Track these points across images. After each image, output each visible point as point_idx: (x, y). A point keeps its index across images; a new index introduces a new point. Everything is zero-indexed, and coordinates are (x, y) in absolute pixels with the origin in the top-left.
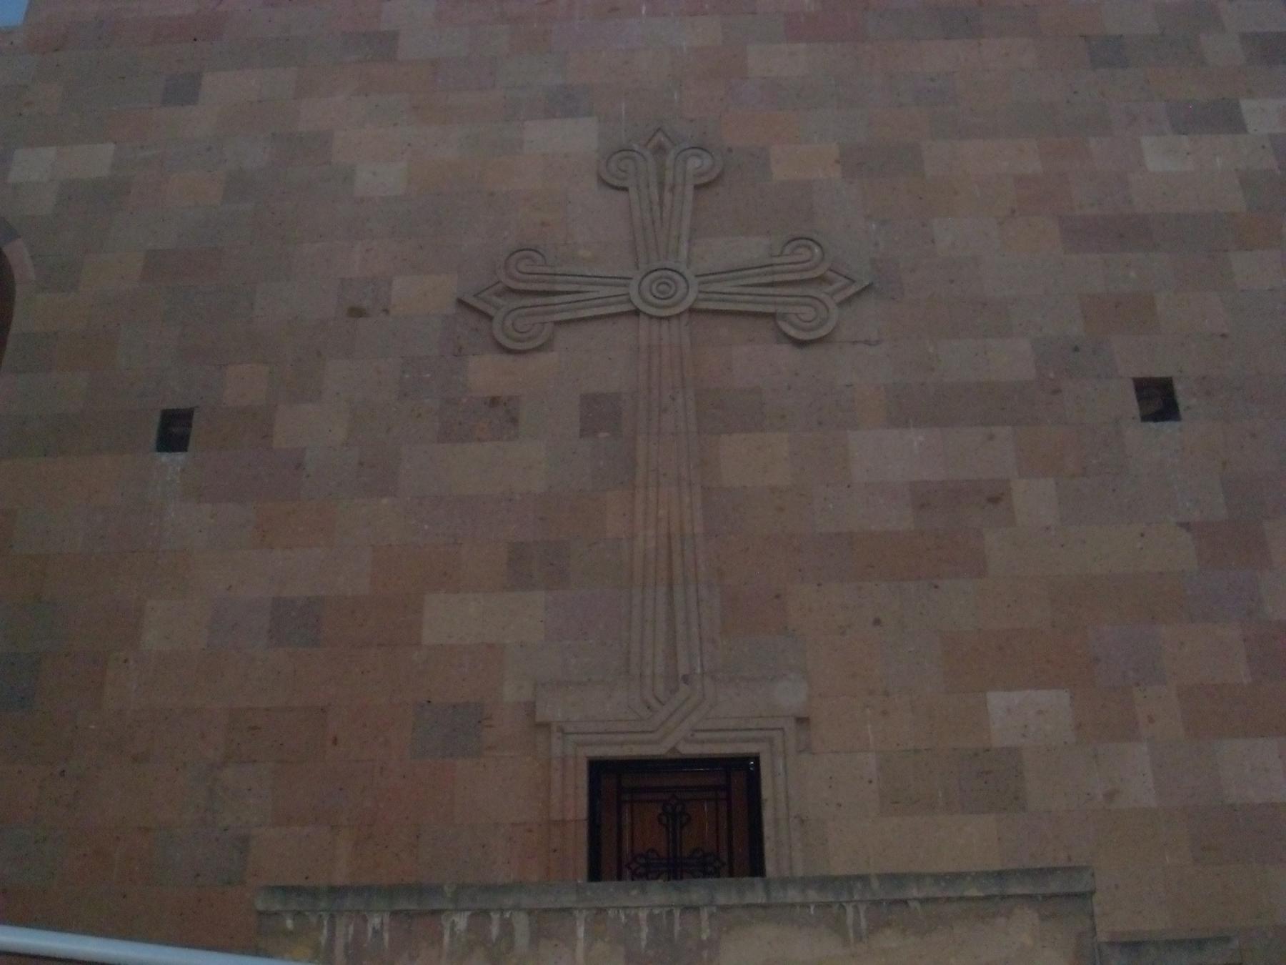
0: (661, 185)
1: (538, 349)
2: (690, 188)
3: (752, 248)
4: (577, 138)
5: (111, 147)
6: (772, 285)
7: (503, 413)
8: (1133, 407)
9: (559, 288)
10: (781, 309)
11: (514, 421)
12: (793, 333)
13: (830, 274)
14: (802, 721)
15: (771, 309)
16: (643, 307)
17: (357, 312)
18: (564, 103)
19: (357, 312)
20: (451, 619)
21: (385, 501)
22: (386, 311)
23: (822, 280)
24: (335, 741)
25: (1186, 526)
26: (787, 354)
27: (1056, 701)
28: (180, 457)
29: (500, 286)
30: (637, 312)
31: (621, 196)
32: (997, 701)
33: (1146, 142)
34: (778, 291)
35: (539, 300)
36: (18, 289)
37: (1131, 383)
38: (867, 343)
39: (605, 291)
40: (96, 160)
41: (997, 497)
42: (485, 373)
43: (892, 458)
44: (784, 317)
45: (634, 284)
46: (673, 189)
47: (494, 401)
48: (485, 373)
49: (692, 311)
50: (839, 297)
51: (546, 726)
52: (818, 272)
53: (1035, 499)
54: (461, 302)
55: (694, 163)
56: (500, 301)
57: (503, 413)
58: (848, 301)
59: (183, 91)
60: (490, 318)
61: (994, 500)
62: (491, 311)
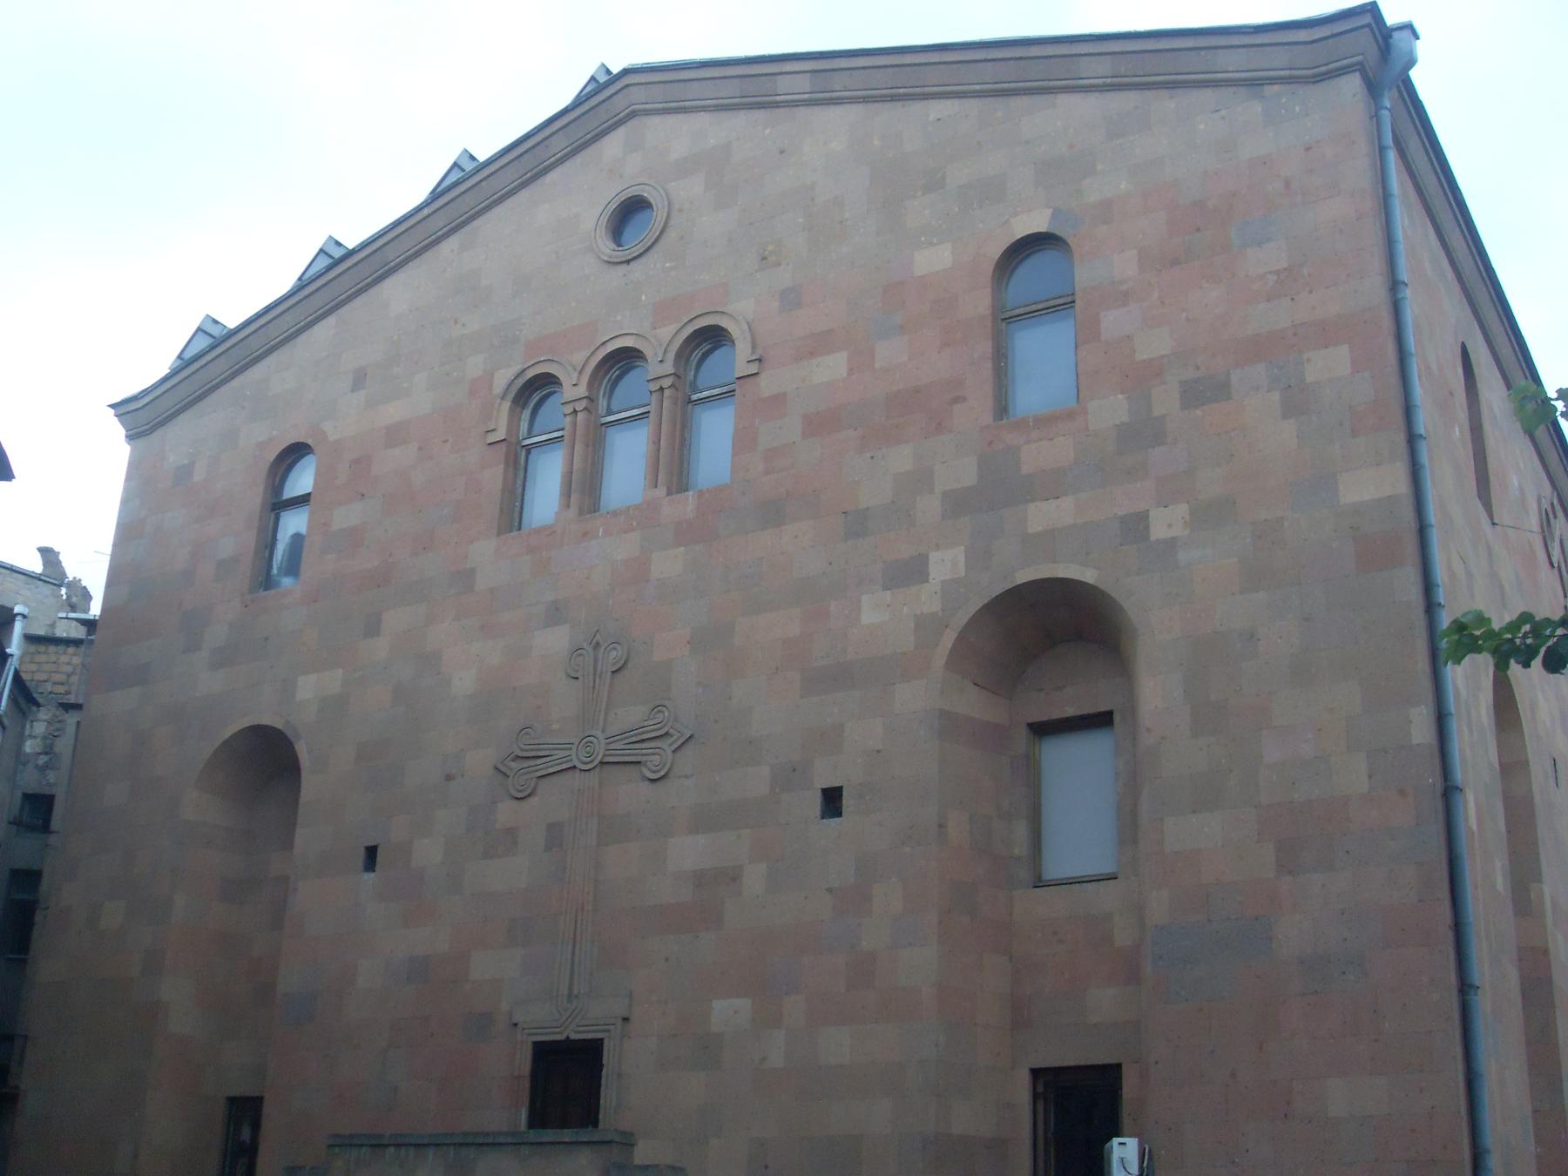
3: (630, 715)
5: (340, 671)
6: (643, 741)
14: (625, 1019)
18: (556, 614)
19: (449, 778)
23: (666, 734)
25: (830, 890)
26: (645, 787)
27: (744, 1003)
28: (372, 875)
32: (717, 1004)
33: (865, 598)
35: (532, 762)
37: (819, 794)
39: (562, 754)
40: (333, 680)
41: (733, 877)
42: (506, 813)
43: (689, 852)
48: (506, 813)
53: (755, 878)
55: (614, 653)
56: (513, 764)
57: (510, 839)
59: (373, 628)
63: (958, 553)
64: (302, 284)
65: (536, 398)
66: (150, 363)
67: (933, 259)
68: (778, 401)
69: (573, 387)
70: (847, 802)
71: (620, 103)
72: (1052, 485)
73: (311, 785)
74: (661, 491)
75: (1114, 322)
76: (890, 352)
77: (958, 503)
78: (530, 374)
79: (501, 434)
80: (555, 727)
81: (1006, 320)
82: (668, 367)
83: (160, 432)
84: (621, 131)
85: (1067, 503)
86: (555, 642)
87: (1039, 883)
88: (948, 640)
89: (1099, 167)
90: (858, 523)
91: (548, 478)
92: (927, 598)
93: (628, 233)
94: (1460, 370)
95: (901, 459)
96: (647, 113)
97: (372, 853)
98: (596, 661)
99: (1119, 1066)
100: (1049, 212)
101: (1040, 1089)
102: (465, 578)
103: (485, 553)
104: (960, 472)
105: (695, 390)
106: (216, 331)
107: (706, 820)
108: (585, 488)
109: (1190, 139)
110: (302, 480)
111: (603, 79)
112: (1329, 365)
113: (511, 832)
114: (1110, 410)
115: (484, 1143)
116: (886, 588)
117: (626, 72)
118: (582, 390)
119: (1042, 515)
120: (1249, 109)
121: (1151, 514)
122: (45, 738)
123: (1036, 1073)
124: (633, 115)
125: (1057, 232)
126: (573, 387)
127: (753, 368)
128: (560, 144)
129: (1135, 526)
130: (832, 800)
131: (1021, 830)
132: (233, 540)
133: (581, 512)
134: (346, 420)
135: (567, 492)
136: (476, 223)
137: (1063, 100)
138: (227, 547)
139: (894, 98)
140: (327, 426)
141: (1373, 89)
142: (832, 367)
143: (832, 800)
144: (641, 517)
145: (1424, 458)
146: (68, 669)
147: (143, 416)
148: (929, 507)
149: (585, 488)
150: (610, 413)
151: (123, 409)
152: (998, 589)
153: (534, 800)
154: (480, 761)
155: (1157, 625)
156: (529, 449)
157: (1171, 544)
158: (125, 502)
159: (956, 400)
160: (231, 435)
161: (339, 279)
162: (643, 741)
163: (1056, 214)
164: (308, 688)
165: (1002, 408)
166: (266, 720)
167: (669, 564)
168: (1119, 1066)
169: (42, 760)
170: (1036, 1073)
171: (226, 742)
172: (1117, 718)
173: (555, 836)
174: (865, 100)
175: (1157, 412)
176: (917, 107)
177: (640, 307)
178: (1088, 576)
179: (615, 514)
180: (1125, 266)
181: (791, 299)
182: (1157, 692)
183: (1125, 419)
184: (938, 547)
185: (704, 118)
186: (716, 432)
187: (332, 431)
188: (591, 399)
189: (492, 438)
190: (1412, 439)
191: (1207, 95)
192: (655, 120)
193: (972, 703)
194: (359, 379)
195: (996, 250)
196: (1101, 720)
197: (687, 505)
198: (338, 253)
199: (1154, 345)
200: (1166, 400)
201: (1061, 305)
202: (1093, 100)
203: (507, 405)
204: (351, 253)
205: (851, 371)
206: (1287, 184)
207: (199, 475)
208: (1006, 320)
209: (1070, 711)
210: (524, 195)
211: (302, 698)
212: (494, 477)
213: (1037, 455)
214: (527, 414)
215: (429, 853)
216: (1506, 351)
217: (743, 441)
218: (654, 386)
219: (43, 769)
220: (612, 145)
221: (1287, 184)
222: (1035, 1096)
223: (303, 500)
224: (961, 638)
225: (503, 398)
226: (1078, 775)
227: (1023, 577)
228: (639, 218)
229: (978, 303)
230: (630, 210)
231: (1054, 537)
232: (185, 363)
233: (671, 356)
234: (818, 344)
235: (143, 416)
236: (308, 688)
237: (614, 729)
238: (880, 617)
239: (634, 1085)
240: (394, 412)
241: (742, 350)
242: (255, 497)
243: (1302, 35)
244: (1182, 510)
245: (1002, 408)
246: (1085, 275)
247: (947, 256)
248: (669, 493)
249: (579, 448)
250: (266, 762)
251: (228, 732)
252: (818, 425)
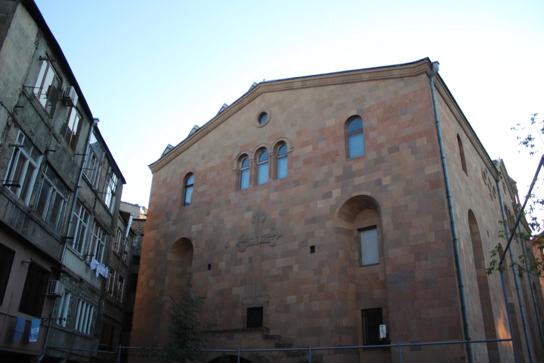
3: (267, 231)
14: (268, 302)
18: (249, 209)
19: (226, 248)
20: (236, 291)
25: (313, 270)
26: (271, 248)
27: (294, 297)
32: (288, 298)
40: (200, 227)
41: (291, 268)
42: (239, 255)
43: (281, 262)
48: (239, 255)
49: (261, 243)
53: (296, 267)
59: (208, 214)
63: (339, 190)
64: (190, 136)
65: (243, 159)
66: (156, 156)
67: (331, 123)
68: (297, 157)
69: (251, 156)
70: (316, 249)
71: (259, 91)
72: (360, 173)
73: (196, 251)
74: (272, 179)
75: (372, 135)
76: (322, 145)
77: (338, 179)
78: (241, 154)
79: (235, 168)
81: (348, 136)
82: (272, 151)
83: (159, 171)
84: (259, 98)
85: (363, 177)
86: (249, 215)
87: (361, 266)
88: (337, 211)
89: (367, 99)
90: (316, 185)
91: (246, 177)
92: (332, 201)
93: (262, 121)
94: (457, 140)
95: (325, 169)
96: (265, 92)
97: (210, 266)
99: (381, 308)
100: (356, 110)
101: (364, 314)
102: (228, 201)
103: (232, 195)
104: (339, 171)
105: (278, 155)
106: (171, 148)
107: (284, 255)
108: (255, 179)
109: (387, 91)
110: (191, 181)
111: (255, 85)
112: (421, 142)
113: (241, 260)
114: (372, 155)
115: (235, 331)
116: (323, 199)
117: (260, 83)
118: (253, 157)
119: (357, 181)
120: (400, 84)
121: (383, 179)
122: (138, 243)
123: (363, 311)
124: (262, 93)
125: (359, 115)
126: (251, 156)
127: (291, 150)
128: (246, 101)
129: (379, 182)
130: (313, 249)
131: (357, 254)
132: (176, 195)
133: (254, 185)
134: (200, 166)
135: (251, 180)
136: (228, 120)
137: (358, 84)
138: (175, 197)
139: (320, 86)
140: (196, 168)
141: (430, 77)
142: (309, 149)
143: (313, 249)
144: (267, 186)
145: (445, 162)
146: (142, 226)
147: (155, 167)
148: (332, 180)
149: (255, 179)
150: (260, 162)
151: (151, 166)
152: (349, 198)
153: (245, 252)
154: (233, 244)
155: (386, 205)
156: (242, 171)
157: (387, 186)
158: (152, 187)
159: (337, 155)
160: (176, 171)
161: (198, 134)
163: (358, 110)
164: (194, 228)
165: (348, 156)
166: (185, 236)
167: (274, 196)
168: (381, 308)
169: (138, 248)
170: (363, 311)
171: (176, 242)
172: (378, 227)
173: (251, 260)
174: (314, 87)
175: (383, 155)
176: (326, 87)
177: (265, 137)
178: (369, 194)
179: (262, 185)
180: (374, 122)
181: (299, 133)
182: (386, 220)
183: (375, 157)
184: (334, 189)
185: (277, 93)
186: (283, 165)
187: (198, 169)
188: (255, 159)
189: (233, 169)
190: (442, 158)
191: (391, 81)
192: (267, 94)
193: (344, 225)
194: (203, 157)
195: (345, 119)
196: (374, 227)
197: (277, 183)
198: (197, 128)
199: (382, 139)
200: (384, 152)
201: (360, 131)
202: (365, 83)
203: (236, 161)
204: (200, 128)
205: (313, 149)
206: (410, 100)
207: (168, 181)
208: (348, 136)
209: (367, 225)
210: (238, 113)
211: (193, 230)
212: (234, 178)
213: (356, 167)
214: (241, 163)
215: (222, 265)
216: (470, 135)
217: (290, 167)
218: (269, 155)
219: (138, 250)
220: (257, 100)
221: (410, 100)
222: (363, 316)
223: (192, 185)
224: (341, 210)
225: (235, 159)
226: (369, 240)
227: (354, 195)
228: (265, 116)
229: (341, 132)
230: (263, 115)
231: (361, 186)
232: (164, 155)
233: (273, 148)
234: (305, 144)
235: (155, 167)
236: (194, 228)
238: (322, 206)
239: (271, 316)
240: (211, 164)
241: (288, 146)
242: (181, 185)
243: (412, 66)
244: (389, 178)
245: (348, 156)
246: (365, 124)
247: (334, 121)
248: (273, 179)
249: (253, 171)
250: (186, 245)
251: (177, 239)
252: (306, 162)
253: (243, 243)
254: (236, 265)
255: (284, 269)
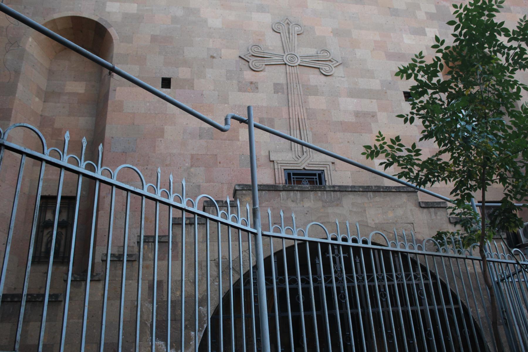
0: (289, 33)
1: (261, 71)
2: (296, 35)
3: (312, 51)
4: (266, 19)
6: (318, 61)
7: (254, 86)
8: (403, 98)
9: (265, 56)
10: (321, 67)
11: (257, 88)
12: (324, 73)
13: (332, 60)
15: (318, 67)
16: (287, 63)
17: (213, 57)
18: (261, 9)
21: (226, 105)
22: (221, 58)
23: (330, 60)
24: (220, 163)
29: (250, 54)
30: (285, 64)
31: (279, 34)
33: (404, 36)
34: (320, 62)
35: (260, 59)
36: (114, 41)
38: (341, 77)
39: (277, 58)
40: (133, 8)
41: (373, 116)
43: (349, 105)
44: (322, 69)
45: (284, 57)
46: (292, 34)
47: (251, 83)
48: (248, 75)
50: (335, 65)
51: (273, 161)
52: (329, 59)
54: (240, 57)
55: (297, 28)
56: (250, 58)
58: (336, 66)
60: (249, 62)
61: (373, 116)
62: (249, 60)
80: (270, 48)
98: (289, 29)
154: (230, 54)
162: (318, 61)
184: (427, 27)
237: (302, 54)
253: (254, 58)
254: (240, 90)
255: (357, 114)
